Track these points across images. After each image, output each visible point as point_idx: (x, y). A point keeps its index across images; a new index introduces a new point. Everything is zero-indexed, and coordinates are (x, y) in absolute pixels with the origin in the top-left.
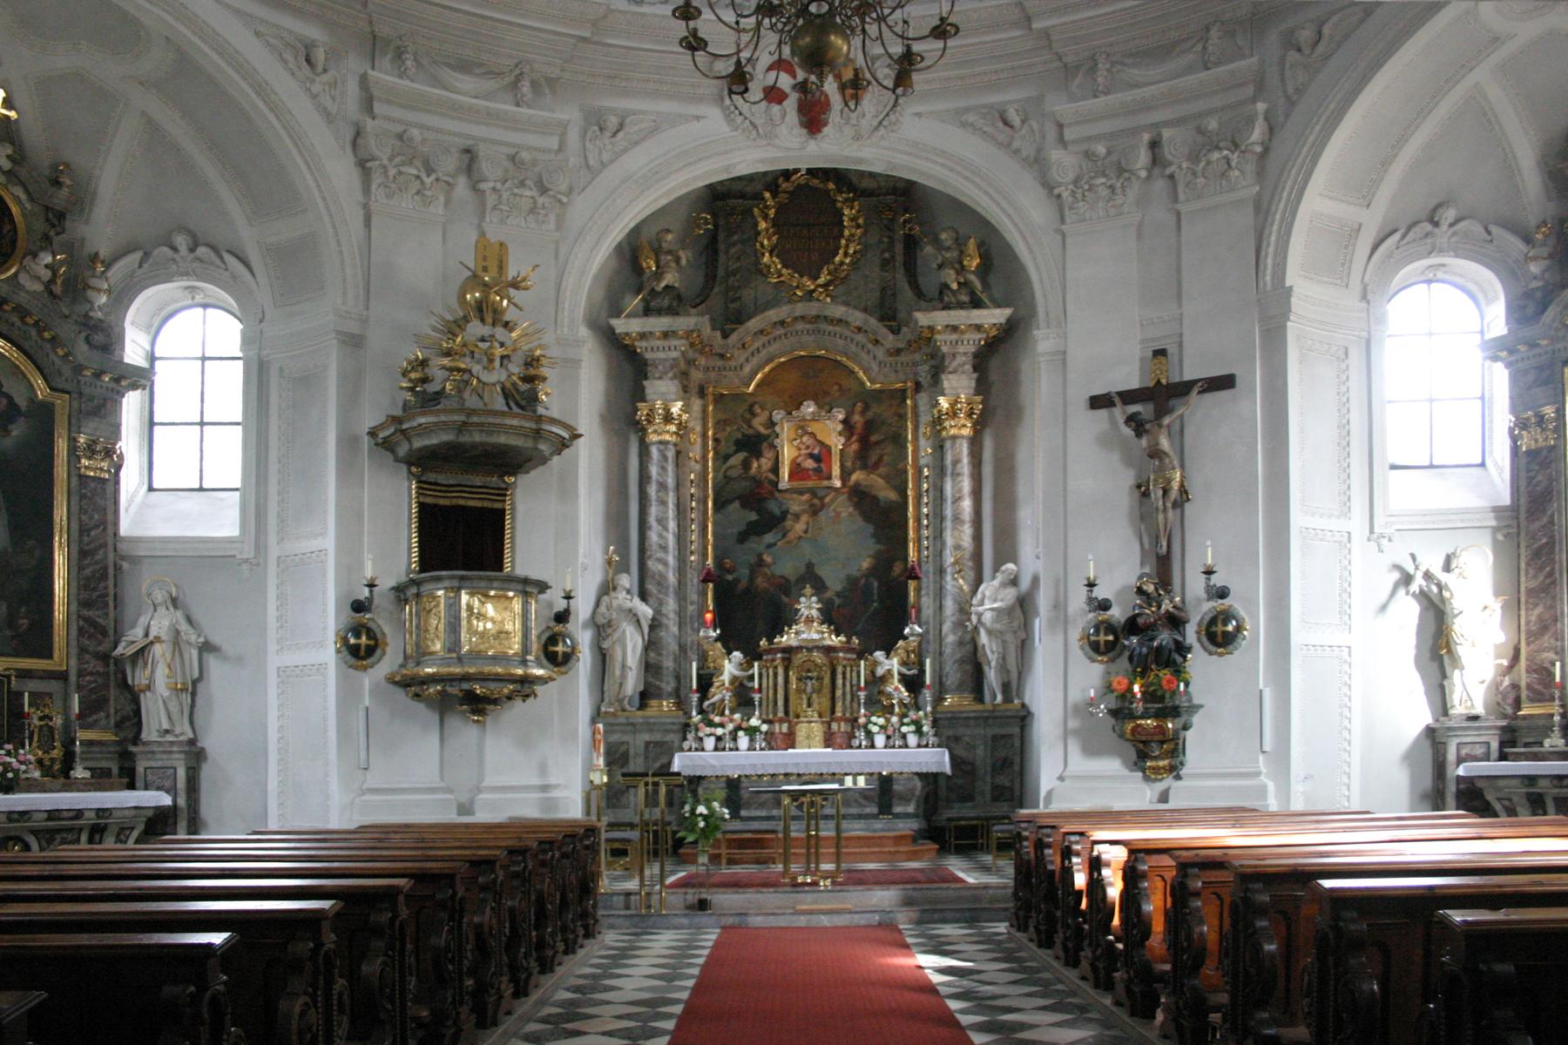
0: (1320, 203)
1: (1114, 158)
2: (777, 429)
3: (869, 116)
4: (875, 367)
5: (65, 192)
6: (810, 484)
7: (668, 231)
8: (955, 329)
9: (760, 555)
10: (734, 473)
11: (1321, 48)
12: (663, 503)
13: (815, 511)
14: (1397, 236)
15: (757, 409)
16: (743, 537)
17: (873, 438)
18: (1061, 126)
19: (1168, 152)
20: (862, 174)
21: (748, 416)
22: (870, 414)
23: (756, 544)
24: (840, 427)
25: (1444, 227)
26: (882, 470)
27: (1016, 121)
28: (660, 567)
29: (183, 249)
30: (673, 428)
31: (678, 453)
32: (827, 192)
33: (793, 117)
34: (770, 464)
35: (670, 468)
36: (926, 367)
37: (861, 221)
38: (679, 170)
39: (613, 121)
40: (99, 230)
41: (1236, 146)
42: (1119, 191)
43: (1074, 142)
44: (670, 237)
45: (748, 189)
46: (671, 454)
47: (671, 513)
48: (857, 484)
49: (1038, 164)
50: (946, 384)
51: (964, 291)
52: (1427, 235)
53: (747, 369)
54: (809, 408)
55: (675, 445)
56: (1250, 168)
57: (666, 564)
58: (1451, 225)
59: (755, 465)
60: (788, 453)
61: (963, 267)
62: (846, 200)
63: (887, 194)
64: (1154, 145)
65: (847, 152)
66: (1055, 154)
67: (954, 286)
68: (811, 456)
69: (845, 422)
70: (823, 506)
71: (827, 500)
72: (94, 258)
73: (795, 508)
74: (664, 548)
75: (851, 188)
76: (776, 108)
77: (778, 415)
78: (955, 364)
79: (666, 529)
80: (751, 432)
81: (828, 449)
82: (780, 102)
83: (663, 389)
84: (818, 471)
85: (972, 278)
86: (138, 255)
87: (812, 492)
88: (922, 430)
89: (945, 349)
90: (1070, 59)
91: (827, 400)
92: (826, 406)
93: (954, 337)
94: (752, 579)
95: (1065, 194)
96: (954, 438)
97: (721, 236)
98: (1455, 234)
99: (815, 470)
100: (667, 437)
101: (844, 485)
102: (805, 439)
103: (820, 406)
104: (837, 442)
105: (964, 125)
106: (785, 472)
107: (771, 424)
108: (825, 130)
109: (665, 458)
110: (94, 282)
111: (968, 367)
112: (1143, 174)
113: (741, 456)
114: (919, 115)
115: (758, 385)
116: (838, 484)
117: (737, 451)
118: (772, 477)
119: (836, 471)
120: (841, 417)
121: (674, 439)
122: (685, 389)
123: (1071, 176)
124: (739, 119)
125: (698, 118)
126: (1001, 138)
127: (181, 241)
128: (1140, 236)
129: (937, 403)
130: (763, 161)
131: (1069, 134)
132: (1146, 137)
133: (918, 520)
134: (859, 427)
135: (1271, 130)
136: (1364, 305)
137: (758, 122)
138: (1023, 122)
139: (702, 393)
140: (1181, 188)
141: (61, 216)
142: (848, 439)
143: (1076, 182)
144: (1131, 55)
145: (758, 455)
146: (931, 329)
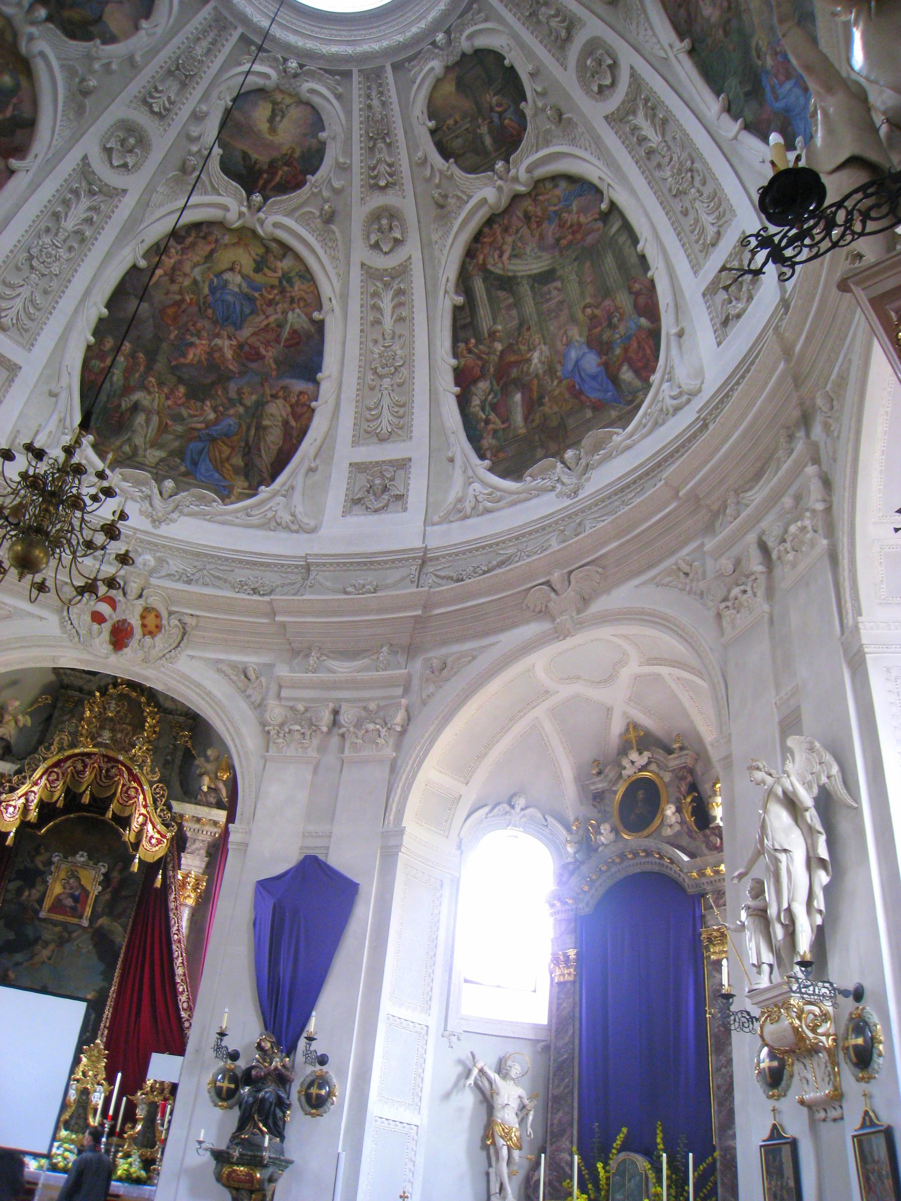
0: (433, 772)
1: (308, 715)
2: (53, 868)
3: (157, 649)
7: (17, 699)
8: (198, 820)
11: (445, 672)
13: (62, 942)
14: (486, 809)
17: (124, 893)
18: (280, 687)
19: (344, 718)
20: (167, 697)
25: (518, 809)
27: (252, 676)
32: (140, 703)
33: (106, 635)
37: (157, 729)
38: (15, 648)
41: (386, 724)
42: (307, 737)
43: (286, 699)
44: (17, 703)
45: (86, 687)
48: (101, 927)
49: (259, 707)
51: (213, 795)
52: (506, 813)
54: (81, 858)
56: (391, 741)
58: (522, 809)
59: (26, 893)
60: (57, 889)
61: (217, 778)
62: (151, 712)
63: (181, 715)
64: (336, 713)
65: (137, 669)
66: (272, 702)
67: (205, 789)
68: (72, 896)
69: (105, 875)
70: (69, 940)
71: (75, 935)
73: (47, 936)
75: (158, 705)
76: (96, 626)
78: (194, 847)
81: (86, 893)
82: (100, 624)
84: (74, 909)
85: (221, 786)
87: (65, 925)
89: (189, 834)
90: (295, 645)
92: (94, 857)
93: (197, 826)
95: (272, 733)
97: (56, 714)
98: (524, 816)
102: (71, 881)
103: (90, 858)
104: (95, 890)
105: (219, 671)
107: (50, 863)
108: (125, 650)
111: (203, 852)
112: (325, 729)
113: (19, 883)
114: (192, 657)
115: (47, 831)
116: (85, 923)
117: (15, 879)
118: (37, 906)
119: (88, 911)
120: (103, 870)
123: (279, 720)
124: (69, 627)
125: (41, 618)
126: (240, 684)
128: (315, 771)
130: (79, 660)
131: (284, 693)
132: (331, 705)
135: (409, 719)
136: (458, 852)
137: (82, 632)
138: (257, 678)
140: (347, 745)
142: (104, 889)
143: (282, 725)
144: (333, 652)
145: (32, 886)
146: (182, 816)
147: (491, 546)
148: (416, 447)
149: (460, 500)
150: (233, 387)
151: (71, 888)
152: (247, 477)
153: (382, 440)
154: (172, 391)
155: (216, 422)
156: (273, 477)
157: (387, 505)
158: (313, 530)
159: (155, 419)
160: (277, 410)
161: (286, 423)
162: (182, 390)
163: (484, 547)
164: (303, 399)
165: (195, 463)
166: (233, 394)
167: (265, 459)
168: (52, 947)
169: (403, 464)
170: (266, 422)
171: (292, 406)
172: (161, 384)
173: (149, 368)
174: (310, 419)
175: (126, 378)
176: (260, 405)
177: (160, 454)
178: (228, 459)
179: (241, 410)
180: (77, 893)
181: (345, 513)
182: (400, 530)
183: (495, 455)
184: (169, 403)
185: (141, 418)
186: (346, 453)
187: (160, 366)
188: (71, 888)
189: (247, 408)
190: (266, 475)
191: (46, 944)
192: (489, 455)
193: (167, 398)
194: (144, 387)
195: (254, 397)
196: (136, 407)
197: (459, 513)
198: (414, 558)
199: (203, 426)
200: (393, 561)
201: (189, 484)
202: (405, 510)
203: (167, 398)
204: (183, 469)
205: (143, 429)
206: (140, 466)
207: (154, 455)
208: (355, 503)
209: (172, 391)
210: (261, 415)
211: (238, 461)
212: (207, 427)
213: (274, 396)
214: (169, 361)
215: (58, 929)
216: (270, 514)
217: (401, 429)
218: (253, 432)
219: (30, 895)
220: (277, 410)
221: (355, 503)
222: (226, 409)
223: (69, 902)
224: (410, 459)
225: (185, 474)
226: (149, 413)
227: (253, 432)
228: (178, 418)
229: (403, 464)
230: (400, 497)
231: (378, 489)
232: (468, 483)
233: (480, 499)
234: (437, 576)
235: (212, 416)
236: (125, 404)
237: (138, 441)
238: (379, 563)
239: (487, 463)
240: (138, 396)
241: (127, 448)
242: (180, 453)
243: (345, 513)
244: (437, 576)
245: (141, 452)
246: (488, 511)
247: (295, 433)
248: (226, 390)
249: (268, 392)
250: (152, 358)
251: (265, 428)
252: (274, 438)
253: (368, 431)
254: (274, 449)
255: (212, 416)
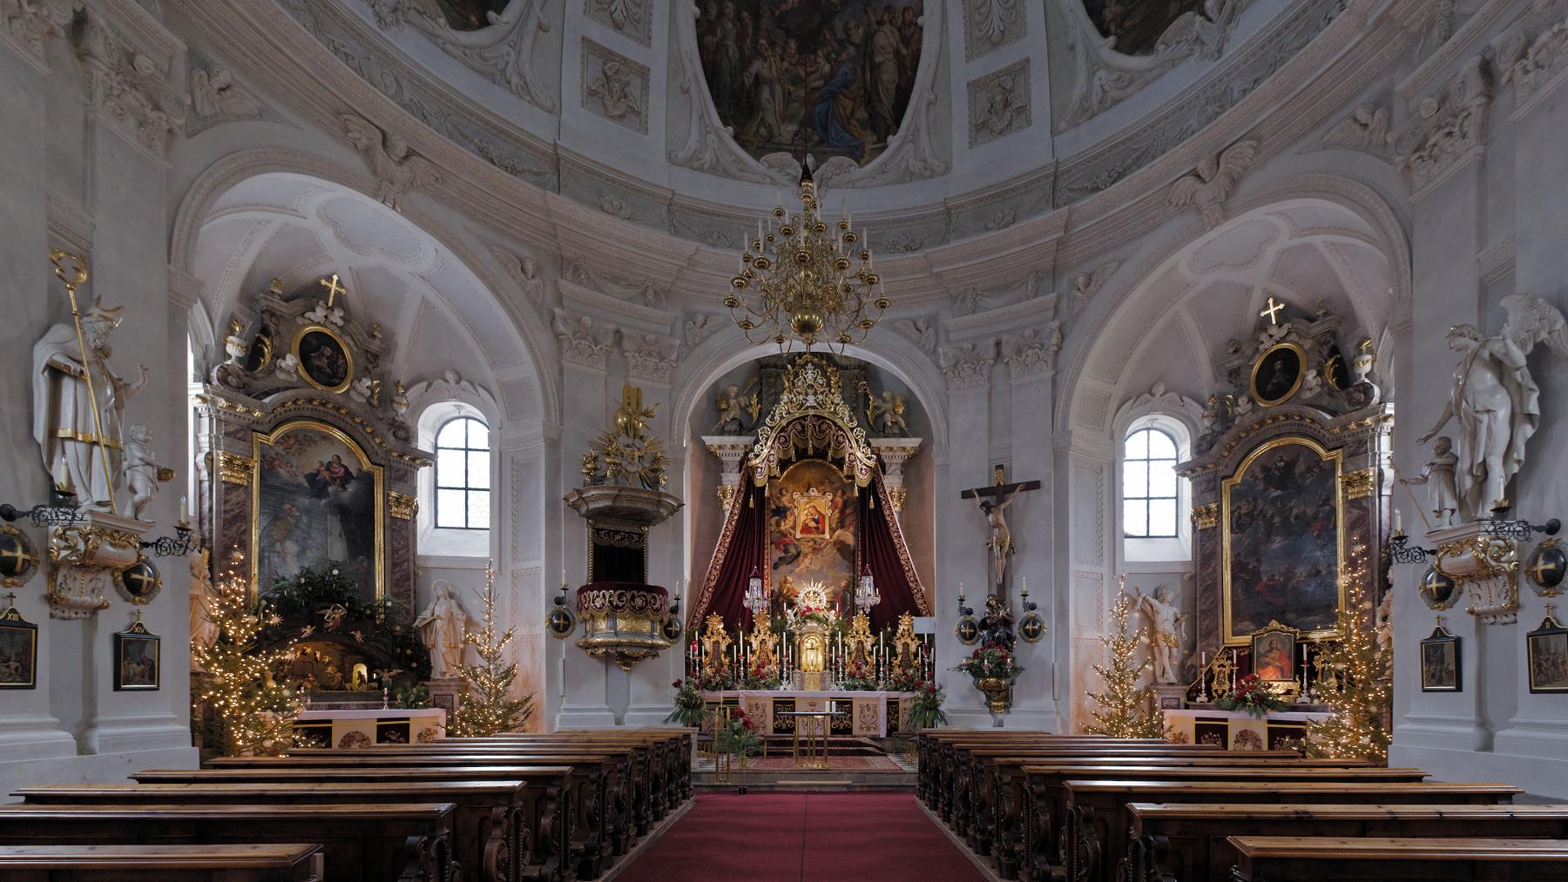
5: (377, 342)
29: (452, 382)
39: (700, 319)
40: (401, 365)
72: (397, 384)
86: (425, 384)
105: (895, 330)
110: (397, 399)
127: (450, 376)
141: (376, 356)
147: (1123, 142)
148: (1032, 45)
149: (1086, 97)
150: (838, 24)
152: (874, 129)
153: (995, 45)
154: (784, 50)
155: (832, 75)
156: (898, 123)
157: (1010, 124)
158: (947, 170)
159: (778, 88)
160: (886, 39)
161: (897, 52)
162: (793, 45)
163: (1116, 146)
164: (909, 16)
165: (825, 129)
166: (841, 35)
167: (887, 102)
169: (1022, 68)
170: (878, 59)
171: (899, 30)
172: (772, 44)
173: (757, 28)
174: (920, 41)
175: (740, 48)
176: (869, 37)
177: (792, 128)
178: (853, 113)
179: (852, 50)
181: (972, 143)
182: (1028, 150)
183: (1120, 26)
184: (786, 64)
185: (765, 93)
186: (964, 70)
187: (766, 22)
189: (857, 46)
190: (890, 122)
192: (1113, 29)
193: (782, 60)
194: (758, 54)
195: (861, 30)
196: (758, 80)
197: (1087, 112)
198: (1046, 177)
199: (820, 83)
200: (1026, 185)
201: (825, 153)
202: (1029, 123)
203: (782, 60)
204: (816, 138)
205: (770, 101)
206: (779, 148)
207: (788, 131)
208: (980, 129)
209: (784, 50)
210: (872, 54)
211: (862, 114)
212: (826, 83)
213: (880, 23)
214: (773, 13)
216: (903, 165)
217: (1012, 28)
218: (868, 76)
220: (886, 39)
221: (980, 129)
222: (838, 54)
224: (1027, 60)
225: (821, 143)
226: (770, 82)
227: (868, 76)
228: (797, 81)
229: (1021, 69)
230: (1023, 110)
231: (1000, 106)
232: (1091, 75)
233: (1107, 88)
234: (1071, 190)
235: (827, 68)
236: (748, 81)
237: (770, 119)
238: (1013, 190)
239: (1112, 39)
240: (757, 66)
241: (763, 131)
242: (807, 122)
243: (972, 143)
244: (1071, 190)
245: (776, 131)
246: (1116, 101)
247: (908, 63)
248: (832, 30)
249: (873, 19)
250: (756, 17)
251: (879, 65)
252: (889, 75)
253: (982, 41)
254: (892, 87)
255: (827, 68)
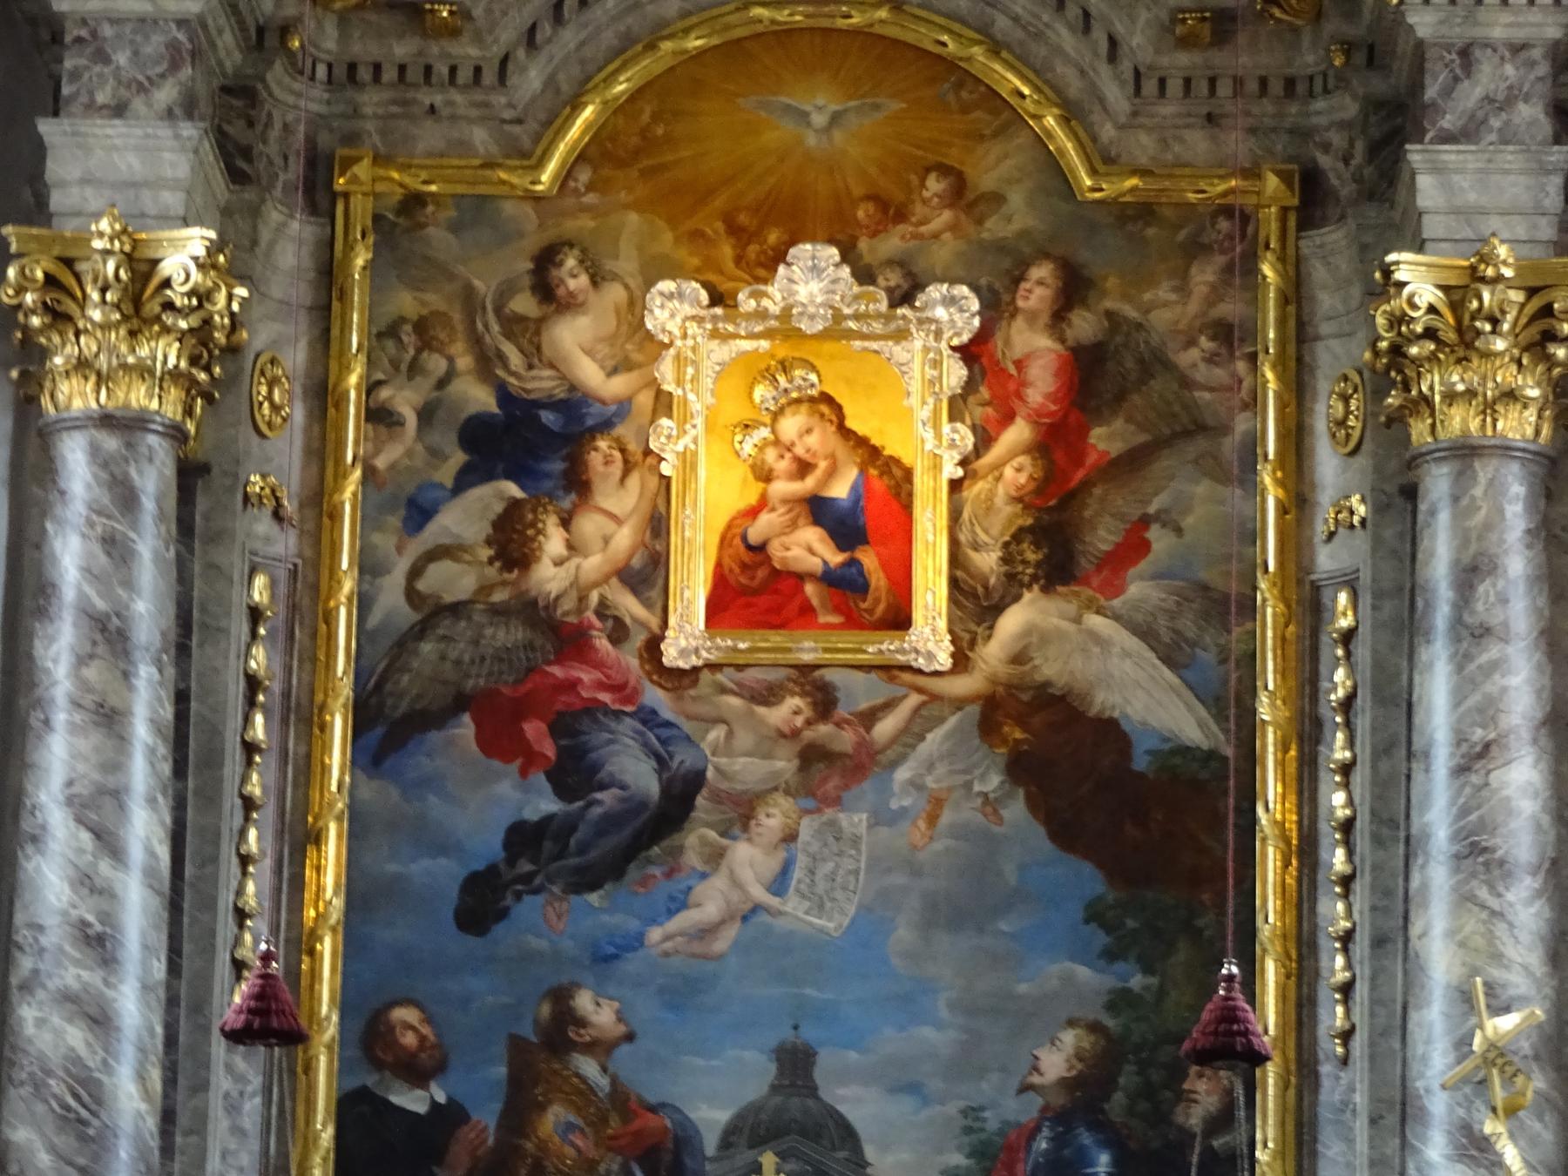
4: (1116, 95)
6: (808, 649)
9: (561, 997)
10: (454, 581)
12: (108, 718)
15: (572, 277)
16: (482, 902)
21: (524, 304)
22: (1084, 325)
23: (546, 923)
24: (955, 373)
26: (1139, 589)
28: (76, 1036)
30: (168, 353)
31: (190, 475)
34: (624, 538)
35: (150, 546)
36: (1349, 107)
46: (153, 478)
47: (143, 770)
50: (1427, 191)
53: (531, 79)
54: (811, 280)
55: (176, 433)
57: (100, 1020)
59: (554, 542)
68: (817, 509)
74: (98, 943)
77: (672, 309)
79: (108, 842)
80: (542, 383)
81: (892, 480)
83: (130, 164)
84: (844, 585)
88: (1325, 409)
91: (892, 243)
94: (520, 1107)
96: (1465, 452)
99: (829, 578)
100: (139, 396)
101: (961, 661)
102: (791, 425)
106: (692, 587)
107: (635, 345)
109: (126, 498)
111: (1532, 114)
117: (466, 479)
121: (170, 406)
122: (237, 161)
129: (1390, 285)
133: (1306, 851)
134: (1041, 385)
139: (318, 195)
151: (803, 468)
168: (772, 819)
180: (840, 490)
188: (803, 468)
191: (741, 812)
215: (790, 710)
219: (572, 559)
223: (809, 548)
